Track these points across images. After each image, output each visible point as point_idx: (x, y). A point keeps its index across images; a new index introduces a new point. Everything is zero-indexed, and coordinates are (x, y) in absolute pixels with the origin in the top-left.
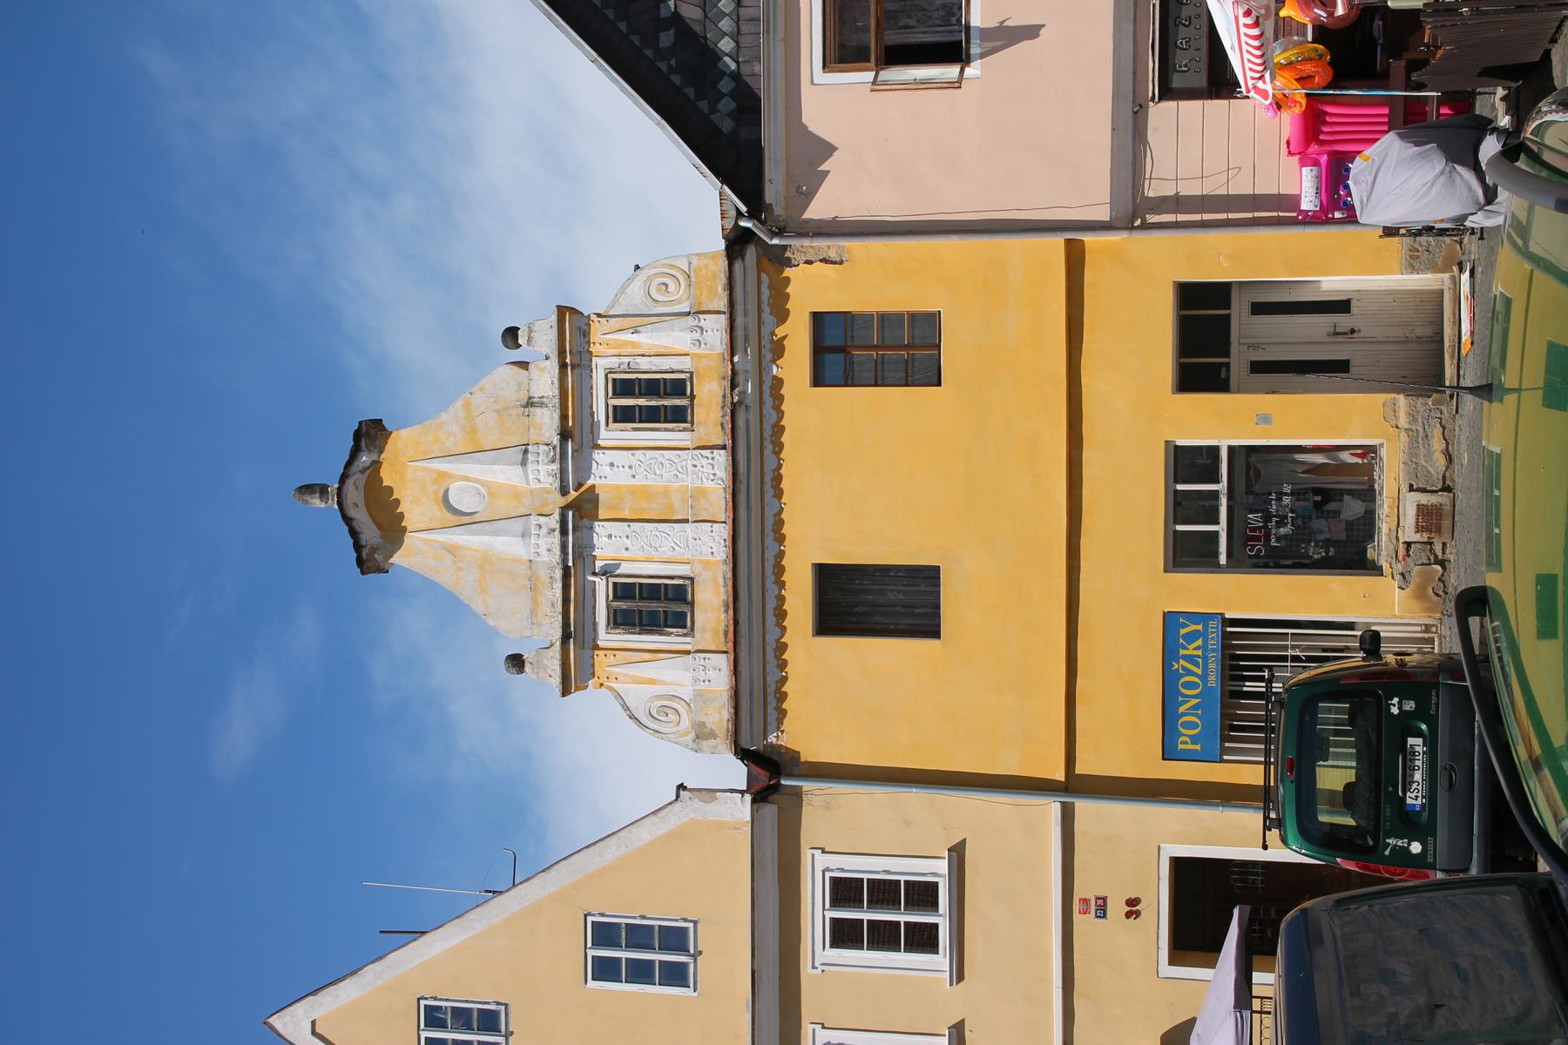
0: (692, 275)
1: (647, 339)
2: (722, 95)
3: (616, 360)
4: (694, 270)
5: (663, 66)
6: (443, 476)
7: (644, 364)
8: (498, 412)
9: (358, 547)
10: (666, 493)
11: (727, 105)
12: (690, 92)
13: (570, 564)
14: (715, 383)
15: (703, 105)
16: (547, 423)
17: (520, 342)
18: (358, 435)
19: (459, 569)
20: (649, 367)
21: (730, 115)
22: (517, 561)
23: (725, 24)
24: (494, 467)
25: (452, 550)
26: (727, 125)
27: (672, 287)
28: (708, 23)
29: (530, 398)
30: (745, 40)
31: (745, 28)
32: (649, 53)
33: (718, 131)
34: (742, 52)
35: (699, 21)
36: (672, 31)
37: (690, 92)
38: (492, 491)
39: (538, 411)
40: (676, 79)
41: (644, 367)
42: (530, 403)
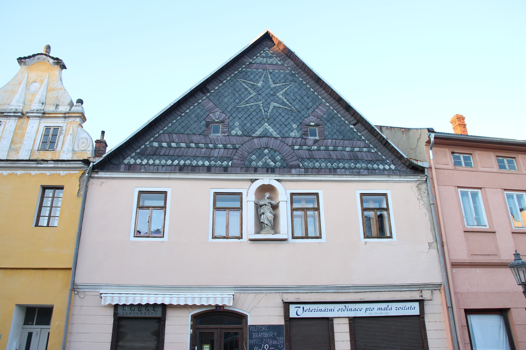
0: (85, 151)
1: (69, 138)
2: (135, 160)
3: (65, 129)
4: (86, 152)
5: (147, 143)
6: (42, 82)
7: (62, 137)
8: (57, 97)
9: (25, 58)
10: (21, 143)
11: (132, 161)
12: (138, 151)
13: (4, 114)
14: (51, 158)
15: (134, 154)
16: (50, 108)
17: (77, 104)
18: (57, 59)
19: (13, 85)
20: (60, 139)
21: (129, 162)
22: (11, 101)
23: (157, 162)
24: (40, 95)
25: (20, 84)
26: (126, 161)
27: (83, 145)
28: (159, 156)
29: (59, 105)
30: (152, 168)
31: (155, 167)
32: (152, 139)
33: (125, 159)
34: (148, 166)
35: (160, 154)
36: (158, 146)
37: (138, 151)
38: (34, 95)
39: (54, 107)
40: (143, 147)
41: (60, 138)
42: (57, 106)
